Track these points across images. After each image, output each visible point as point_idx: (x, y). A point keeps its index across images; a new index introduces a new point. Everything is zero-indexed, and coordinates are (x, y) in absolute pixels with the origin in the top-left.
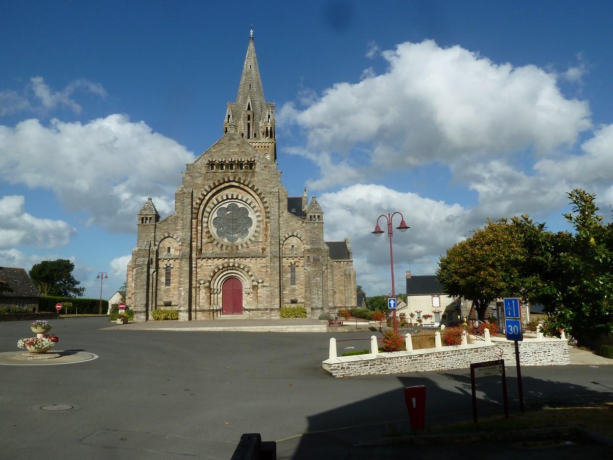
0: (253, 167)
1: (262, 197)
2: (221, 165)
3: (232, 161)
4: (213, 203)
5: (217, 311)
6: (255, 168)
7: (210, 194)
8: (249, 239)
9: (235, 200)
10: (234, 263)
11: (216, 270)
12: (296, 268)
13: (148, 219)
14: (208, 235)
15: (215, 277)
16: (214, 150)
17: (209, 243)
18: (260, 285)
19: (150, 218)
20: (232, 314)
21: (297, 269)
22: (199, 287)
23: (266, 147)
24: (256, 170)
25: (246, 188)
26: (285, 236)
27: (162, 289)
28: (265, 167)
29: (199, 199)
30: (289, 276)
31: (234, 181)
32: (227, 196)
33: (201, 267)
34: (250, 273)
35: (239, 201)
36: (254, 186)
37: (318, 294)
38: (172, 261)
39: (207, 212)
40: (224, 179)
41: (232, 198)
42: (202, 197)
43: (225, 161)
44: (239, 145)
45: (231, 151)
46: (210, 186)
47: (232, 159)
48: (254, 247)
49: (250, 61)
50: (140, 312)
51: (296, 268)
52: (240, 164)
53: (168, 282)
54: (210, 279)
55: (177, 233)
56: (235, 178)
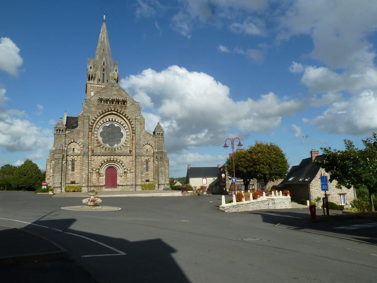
0: (125, 104)
1: (130, 121)
2: (107, 101)
3: (113, 99)
4: (101, 123)
5: (102, 186)
6: (126, 104)
7: (100, 118)
8: (122, 145)
9: (113, 122)
10: (114, 159)
11: (103, 163)
12: (149, 162)
13: (61, 130)
14: (97, 142)
15: (102, 166)
16: (102, 92)
17: (98, 146)
18: (128, 171)
19: (62, 130)
21: (149, 163)
22: (92, 172)
23: (96, 87)
24: (128, 105)
25: (121, 115)
26: (143, 144)
27: (69, 174)
28: (132, 104)
29: (93, 120)
30: (145, 166)
31: (114, 111)
32: (109, 119)
33: (93, 161)
34: (123, 165)
36: (126, 115)
37: (162, 177)
38: (75, 157)
39: (97, 128)
40: (108, 109)
41: (112, 121)
42: (95, 119)
43: (109, 99)
44: (117, 90)
45: (113, 93)
46: (100, 113)
47: (113, 98)
49: (103, 35)
50: (58, 187)
51: (149, 162)
52: (118, 101)
53: (73, 169)
54: (99, 168)
55: (79, 140)
56: (115, 109)
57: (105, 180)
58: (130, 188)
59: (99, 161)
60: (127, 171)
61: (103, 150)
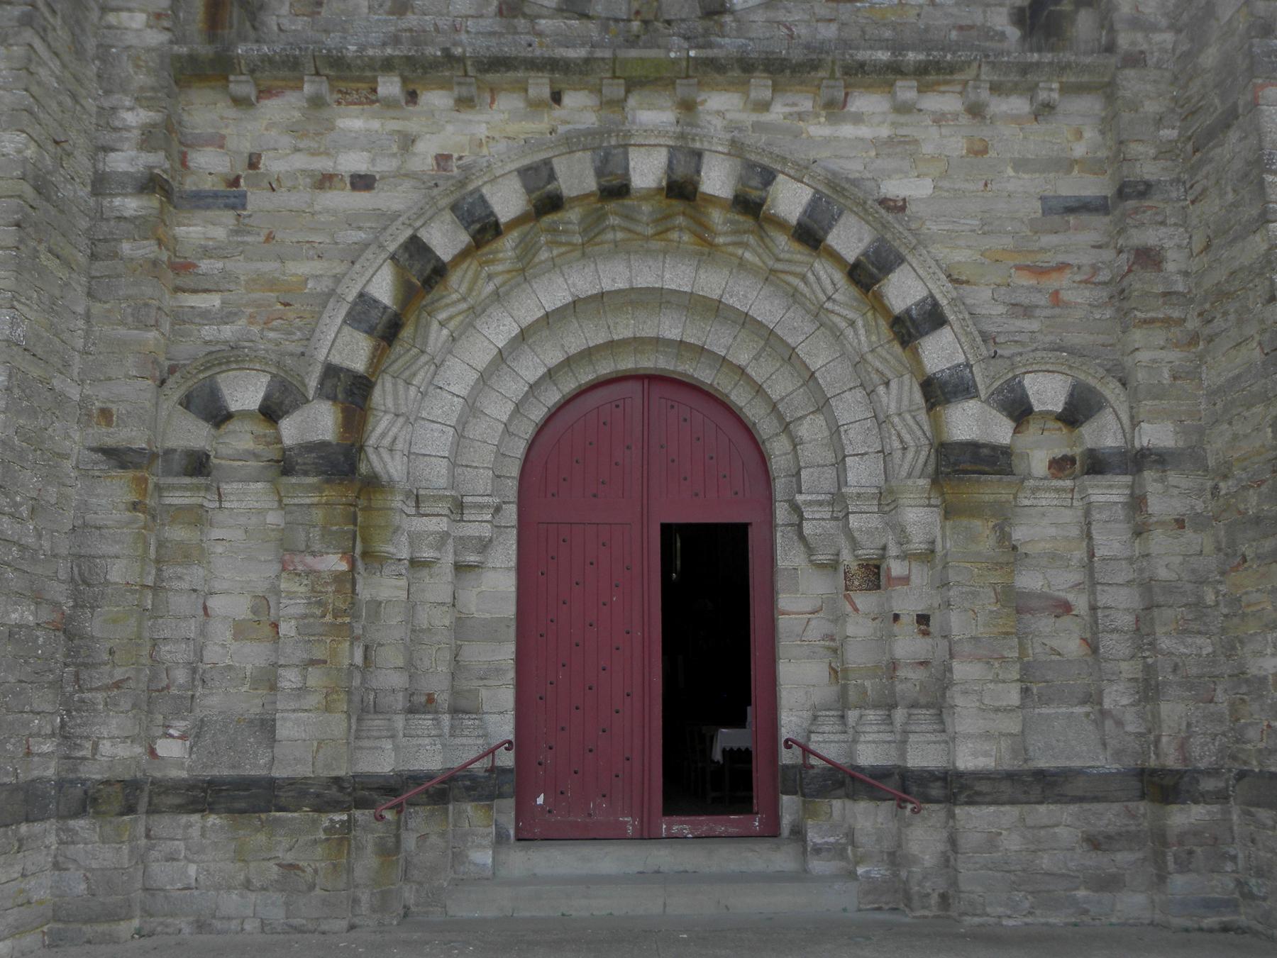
20: (647, 835)
57: (507, 652)
58: (1095, 843)
59: (342, 199)
60: (1001, 431)
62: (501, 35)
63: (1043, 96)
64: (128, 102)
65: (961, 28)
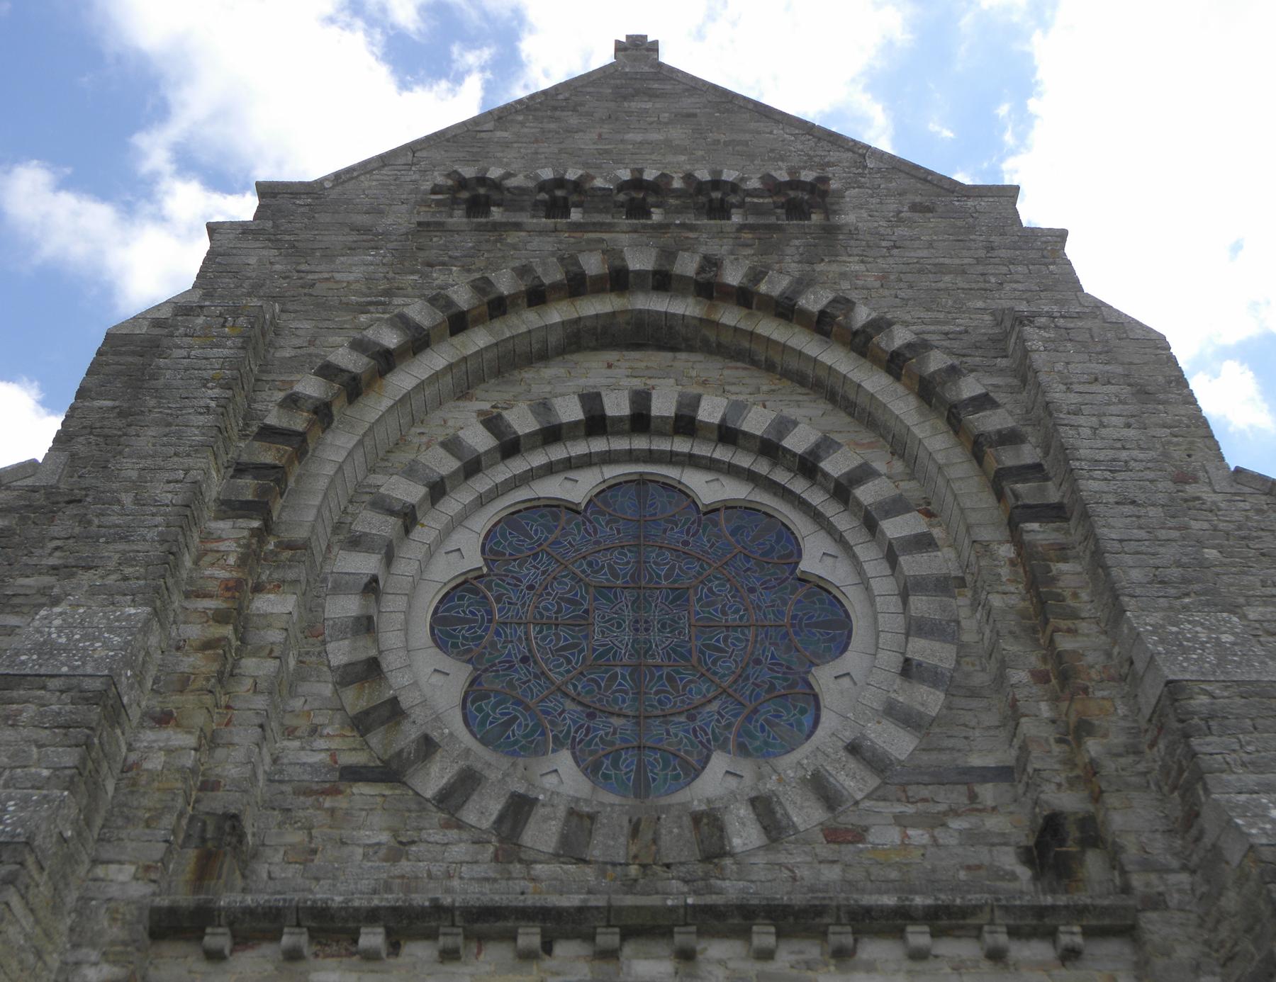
8: (854, 749)
14: (355, 700)
17: (353, 774)
24: (848, 218)
31: (662, 281)
35: (702, 450)
45: (630, 136)
48: (918, 836)
61: (460, 851)
62: (495, 880)
63: (1065, 940)
64: (94, 956)
65: (969, 868)
